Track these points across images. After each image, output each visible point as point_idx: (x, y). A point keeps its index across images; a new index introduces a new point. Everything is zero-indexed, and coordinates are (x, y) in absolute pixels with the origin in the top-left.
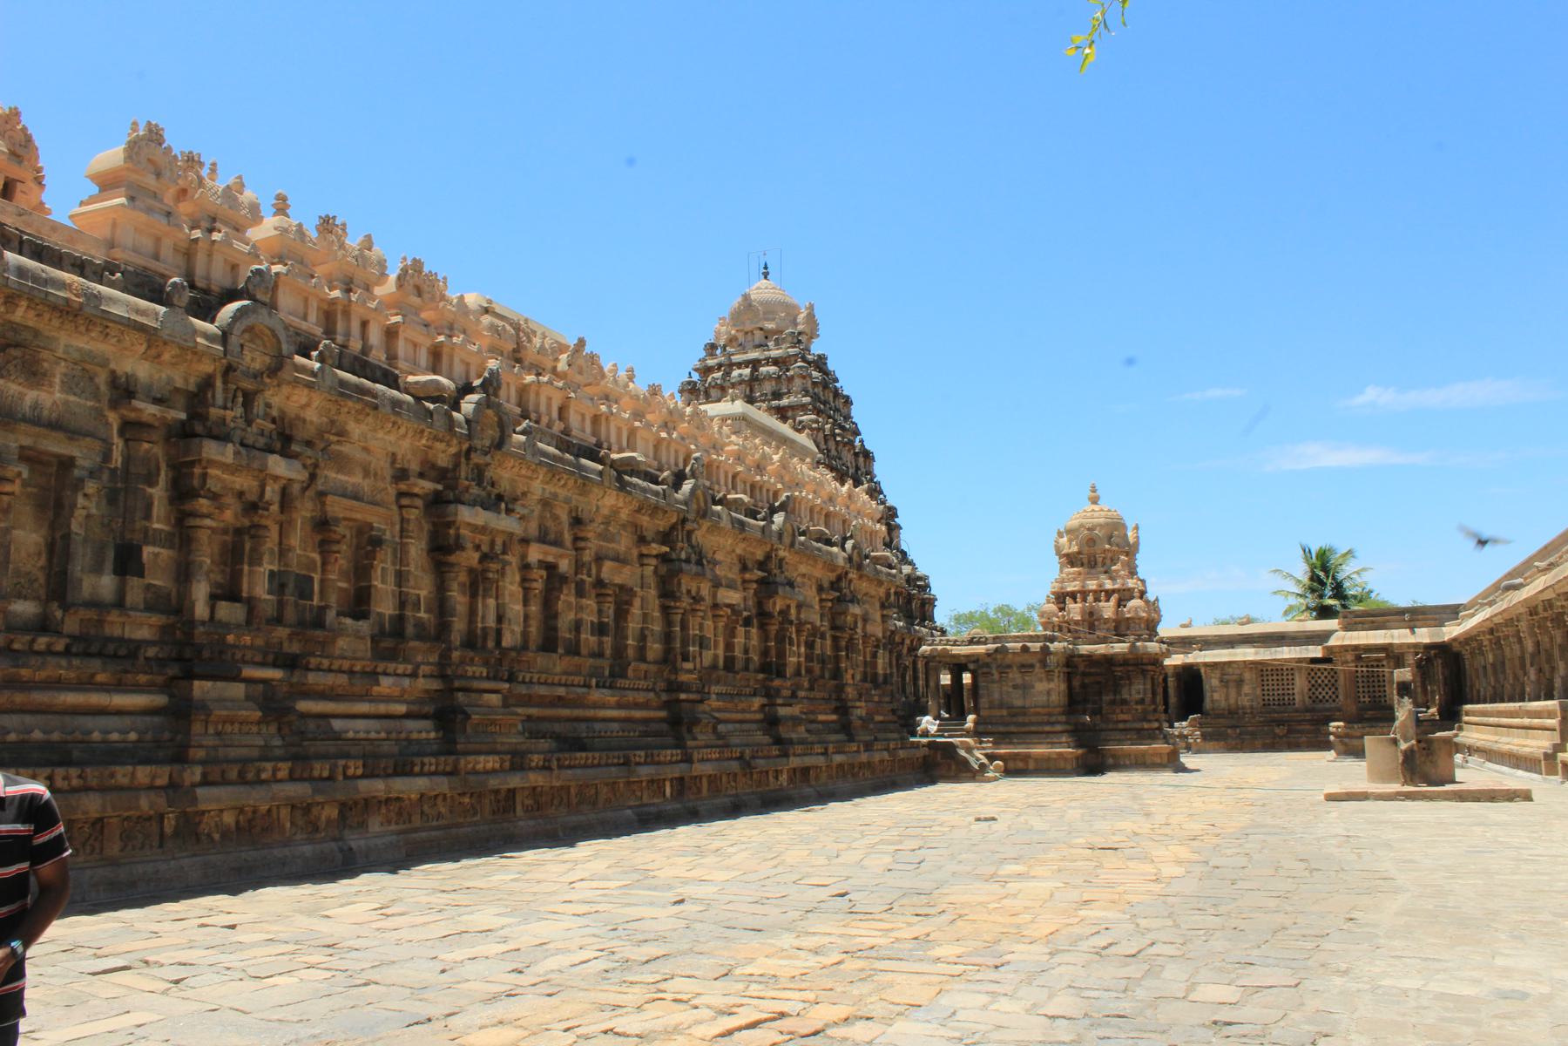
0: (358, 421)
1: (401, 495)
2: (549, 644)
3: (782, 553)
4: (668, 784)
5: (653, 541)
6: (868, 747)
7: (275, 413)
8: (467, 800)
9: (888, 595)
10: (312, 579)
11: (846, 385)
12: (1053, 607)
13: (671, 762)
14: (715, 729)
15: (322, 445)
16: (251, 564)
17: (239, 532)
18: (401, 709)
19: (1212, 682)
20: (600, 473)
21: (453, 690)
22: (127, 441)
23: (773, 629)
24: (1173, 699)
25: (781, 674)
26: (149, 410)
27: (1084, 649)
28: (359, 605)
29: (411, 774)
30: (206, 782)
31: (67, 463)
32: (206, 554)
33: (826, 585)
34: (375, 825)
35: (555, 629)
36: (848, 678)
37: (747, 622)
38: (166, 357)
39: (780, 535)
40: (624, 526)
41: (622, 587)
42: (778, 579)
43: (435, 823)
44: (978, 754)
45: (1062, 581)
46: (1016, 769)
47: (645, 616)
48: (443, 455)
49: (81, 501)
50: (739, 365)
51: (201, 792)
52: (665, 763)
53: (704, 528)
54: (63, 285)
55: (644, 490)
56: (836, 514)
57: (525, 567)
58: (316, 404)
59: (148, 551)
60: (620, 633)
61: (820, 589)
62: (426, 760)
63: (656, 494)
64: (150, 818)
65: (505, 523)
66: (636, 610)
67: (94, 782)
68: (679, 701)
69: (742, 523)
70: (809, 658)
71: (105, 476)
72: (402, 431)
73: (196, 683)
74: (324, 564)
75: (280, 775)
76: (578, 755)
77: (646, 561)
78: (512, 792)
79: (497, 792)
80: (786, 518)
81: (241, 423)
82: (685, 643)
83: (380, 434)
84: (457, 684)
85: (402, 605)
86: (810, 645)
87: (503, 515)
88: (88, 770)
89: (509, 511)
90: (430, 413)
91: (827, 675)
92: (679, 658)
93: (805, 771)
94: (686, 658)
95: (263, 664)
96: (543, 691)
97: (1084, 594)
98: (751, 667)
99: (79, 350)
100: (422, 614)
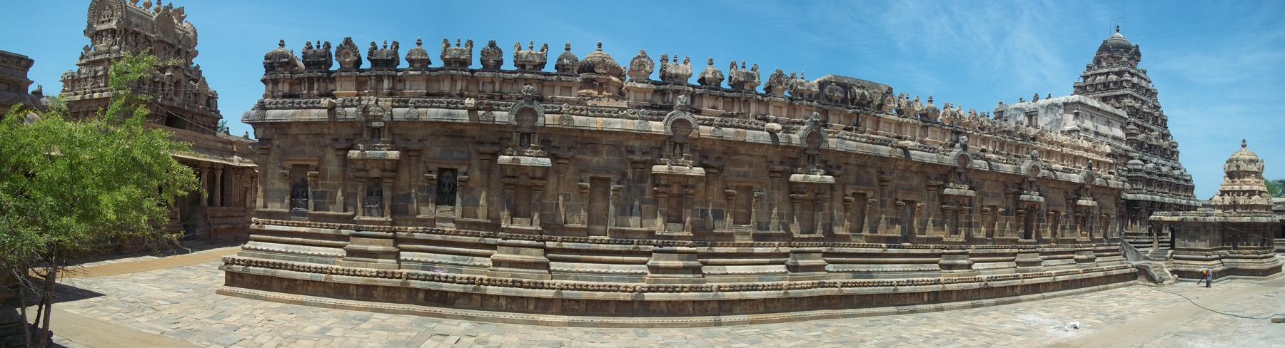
50: (1100, 74)
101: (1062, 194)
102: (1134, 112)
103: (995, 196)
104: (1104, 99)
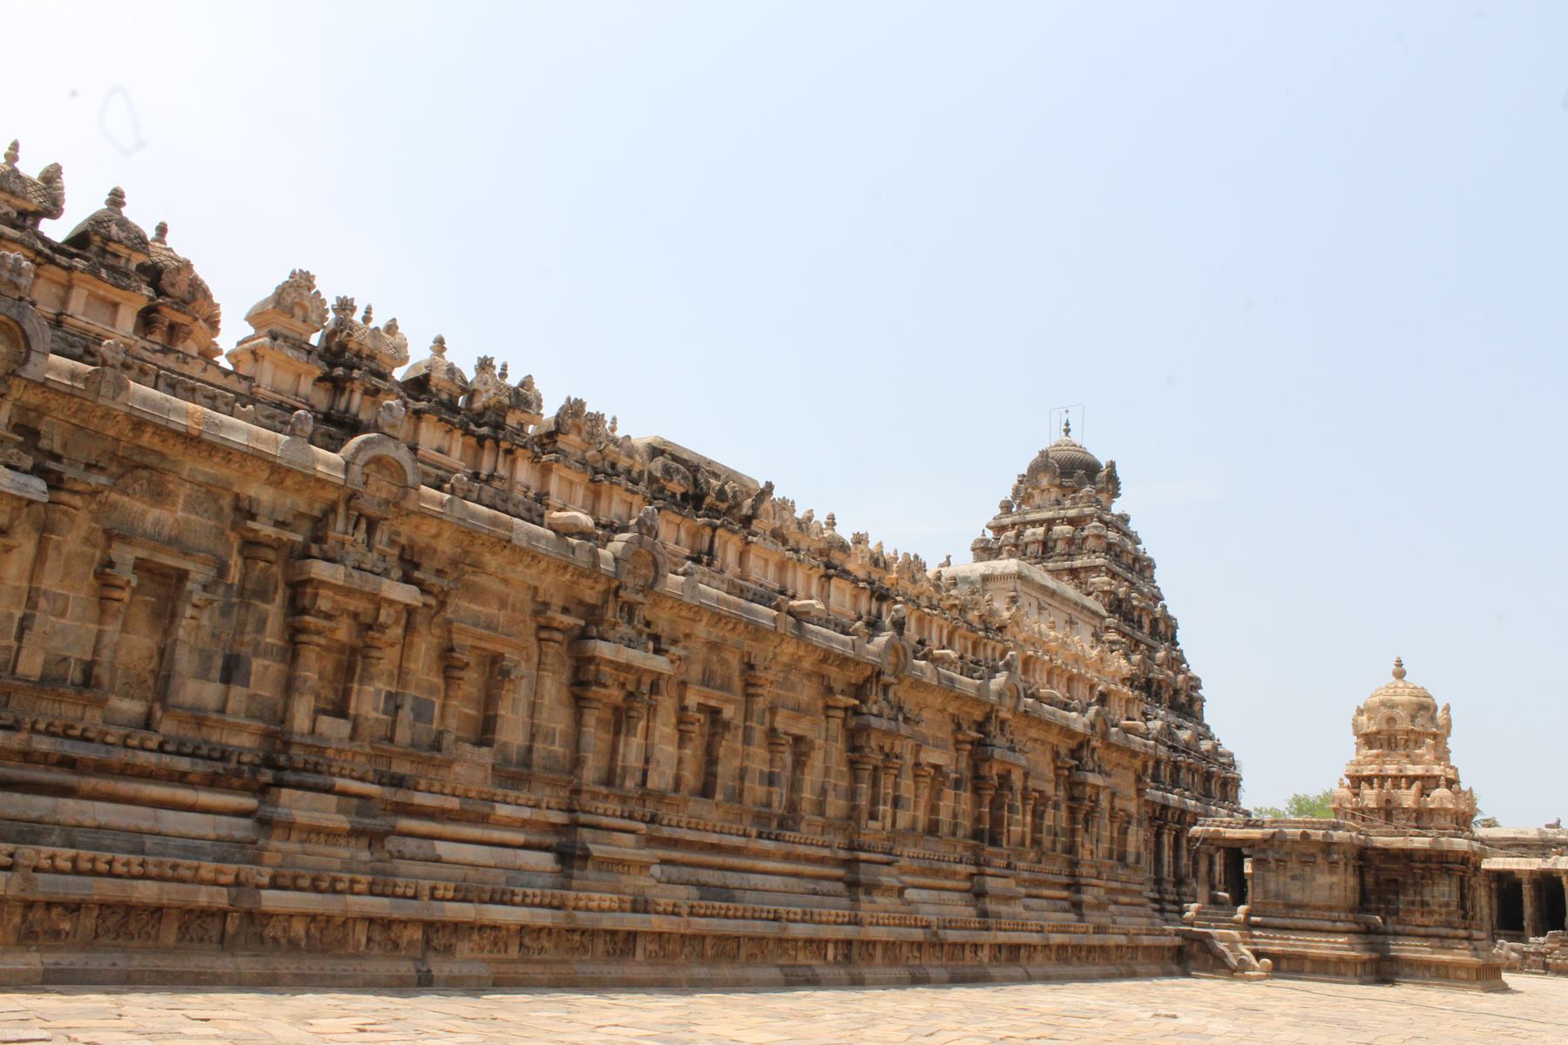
0: (494, 554)
3: (1004, 714)
4: (831, 948)
5: (843, 692)
6: (1100, 929)
7: (403, 540)
8: (577, 937)
9: (1145, 767)
11: (1150, 546)
12: (1346, 793)
13: (835, 923)
14: (901, 892)
15: (455, 575)
16: (361, 683)
17: (354, 651)
18: (520, 838)
20: (775, 619)
21: (576, 825)
22: (245, 558)
23: (988, 794)
25: (994, 841)
26: (265, 529)
27: (1380, 841)
28: (485, 732)
29: (513, 904)
30: (274, 885)
31: (183, 575)
32: (312, 669)
33: (1063, 751)
34: (464, 948)
35: (714, 776)
36: (1084, 854)
37: (957, 785)
38: (289, 482)
39: (1000, 695)
40: (809, 675)
41: (798, 739)
42: (996, 742)
43: (536, 957)
44: (1244, 949)
45: (1359, 763)
46: (1286, 966)
47: (827, 772)
48: (590, 595)
49: (189, 611)
50: (1033, 523)
51: (265, 893)
52: (828, 923)
53: (907, 683)
54: (187, 414)
55: (828, 639)
56: (1080, 677)
57: (684, 709)
58: (447, 534)
59: (257, 664)
60: (795, 786)
61: (1056, 755)
62: (529, 891)
63: (844, 644)
64: (213, 914)
65: (660, 664)
66: (817, 760)
67: (153, 870)
68: (858, 861)
69: (951, 680)
70: (1037, 828)
71: (221, 590)
72: (543, 565)
73: (285, 791)
74: (446, 690)
75: (358, 887)
76: (717, 904)
77: (831, 713)
78: (632, 936)
79: (614, 933)
80: (1008, 678)
81: (362, 548)
82: (874, 801)
83: (520, 568)
84: (583, 818)
85: (533, 737)
86: (1038, 815)
87: (651, 654)
88: (150, 859)
89: (657, 651)
90: (573, 549)
91: (1059, 847)
92: (865, 816)
93: (1015, 949)
94: (873, 816)
95: (361, 779)
97: (1383, 778)
98: (960, 833)
99: (205, 474)
101: (1049, 756)
102: (1117, 606)
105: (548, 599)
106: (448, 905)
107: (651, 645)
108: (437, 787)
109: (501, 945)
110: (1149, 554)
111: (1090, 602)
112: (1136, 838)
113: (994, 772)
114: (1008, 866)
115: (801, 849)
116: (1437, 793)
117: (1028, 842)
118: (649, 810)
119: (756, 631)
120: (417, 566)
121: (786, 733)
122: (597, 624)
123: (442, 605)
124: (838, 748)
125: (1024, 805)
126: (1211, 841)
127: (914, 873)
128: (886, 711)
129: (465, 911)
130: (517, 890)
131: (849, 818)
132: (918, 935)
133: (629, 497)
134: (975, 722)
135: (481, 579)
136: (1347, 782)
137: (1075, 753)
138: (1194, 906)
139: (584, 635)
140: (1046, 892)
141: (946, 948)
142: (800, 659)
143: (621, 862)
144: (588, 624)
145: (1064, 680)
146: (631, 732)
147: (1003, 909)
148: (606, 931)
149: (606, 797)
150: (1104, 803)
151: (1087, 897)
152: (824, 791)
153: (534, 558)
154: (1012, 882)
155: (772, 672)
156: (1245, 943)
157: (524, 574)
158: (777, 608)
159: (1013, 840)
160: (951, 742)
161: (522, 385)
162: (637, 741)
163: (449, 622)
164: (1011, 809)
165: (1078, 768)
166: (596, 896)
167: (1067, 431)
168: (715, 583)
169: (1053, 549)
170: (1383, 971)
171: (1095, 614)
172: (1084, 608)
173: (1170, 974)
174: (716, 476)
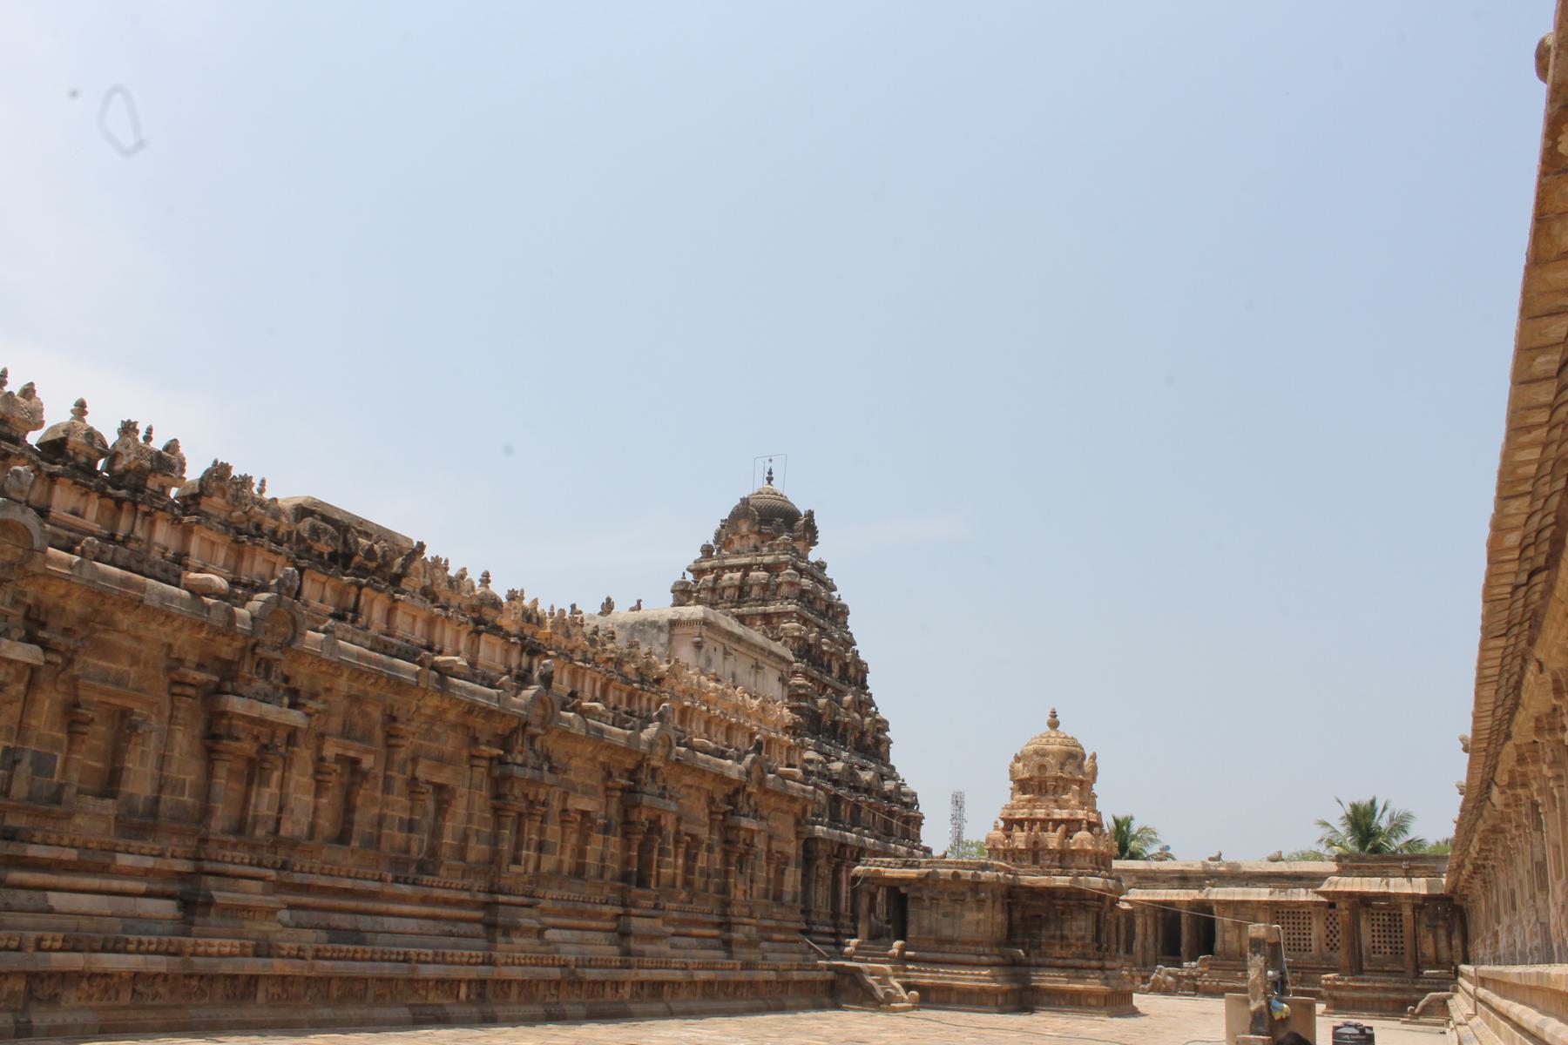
1: (175, 683)
2: (342, 837)
3: (654, 763)
5: (488, 743)
6: (748, 966)
7: (29, 600)
10: (55, 757)
11: (844, 593)
12: (1000, 834)
13: (468, 963)
14: (540, 933)
18: (141, 886)
19: (1224, 921)
20: (417, 674)
23: (637, 838)
24: (1185, 937)
25: (642, 882)
28: (110, 783)
29: (126, 952)
33: (719, 797)
36: (738, 894)
37: (606, 829)
39: (651, 744)
40: (454, 727)
41: (440, 788)
43: (150, 1002)
44: (894, 982)
45: (1012, 807)
46: (932, 998)
48: (227, 650)
50: (732, 568)
52: (461, 964)
53: (555, 733)
55: (473, 693)
56: (739, 726)
57: (322, 759)
58: (76, 595)
60: (436, 833)
61: (711, 801)
62: (145, 939)
63: (489, 697)
65: (296, 718)
66: (460, 807)
68: (497, 903)
69: (600, 731)
70: (689, 870)
72: (177, 624)
74: (71, 742)
76: (344, 947)
77: (476, 762)
78: (253, 980)
79: (234, 977)
82: (518, 846)
83: (154, 626)
84: (208, 866)
85: (160, 789)
86: (690, 857)
87: (285, 709)
90: (208, 608)
91: (712, 888)
94: (516, 860)
96: (323, 881)
97: (1033, 821)
98: (608, 875)
100: (186, 798)
101: (703, 802)
102: (806, 651)
103: (587, 792)
104: (741, 619)
105: (182, 656)
106: (54, 955)
107: (286, 700)
108: (54, 838)
109: (112, 993)
110: (843, 601)
111: (777, 647)
112: (792, 879)
113: (643, 817)
114: (656, 907)
115: (438, 893)
116: (1079, 835)
117: (679, 883)
118: (281, 856)
119: (398, 685)
120: (43, 626)
121: (428, 782)
122: (232, 679)
123: (70, 662)
124: (482, 797)
125: (676, 848)
126: (875, 880)
127: (557, 915)
128: (531, 762)
129: (76, 961)
130: (131, 937)
131: (491, 862)
132: (555, 973)
133: (272, 558)
134: (627, 770)
135: (112, 637)
136: (1001, 824)
137: (730, 799)
138: (854, 941)
139: (219, 691)
140: (696, 931)
141: (585, 986)
142: (445, 711)
143: (246, 908)
144: (223, 679)
145: (723, 729)
146: (265, 782)
147: (648, 948)
148: (226, 976)
149: (234, 846)
150: (760, 844)
151: (737, 935)
152: (465, 837)
153: (167, 617)
154: (659, 923)
155: (415, 724)
156: (897, 977)
157: (158, 631)
158: (421, 663)
159: (663, 881)
160: (601, 789)
161: (167, 448)
162: (272, 790)
163: (75, 679)
164: (662, 852)
165: (732, 813)
166: (216, 942)
167: (770, 480)
168: (357, 639)
169: (748, 594)
170: (1024, 1000)
171: (782, 659)
172: (771, 653)
173: (820, 1007)
174: (367, 535)
